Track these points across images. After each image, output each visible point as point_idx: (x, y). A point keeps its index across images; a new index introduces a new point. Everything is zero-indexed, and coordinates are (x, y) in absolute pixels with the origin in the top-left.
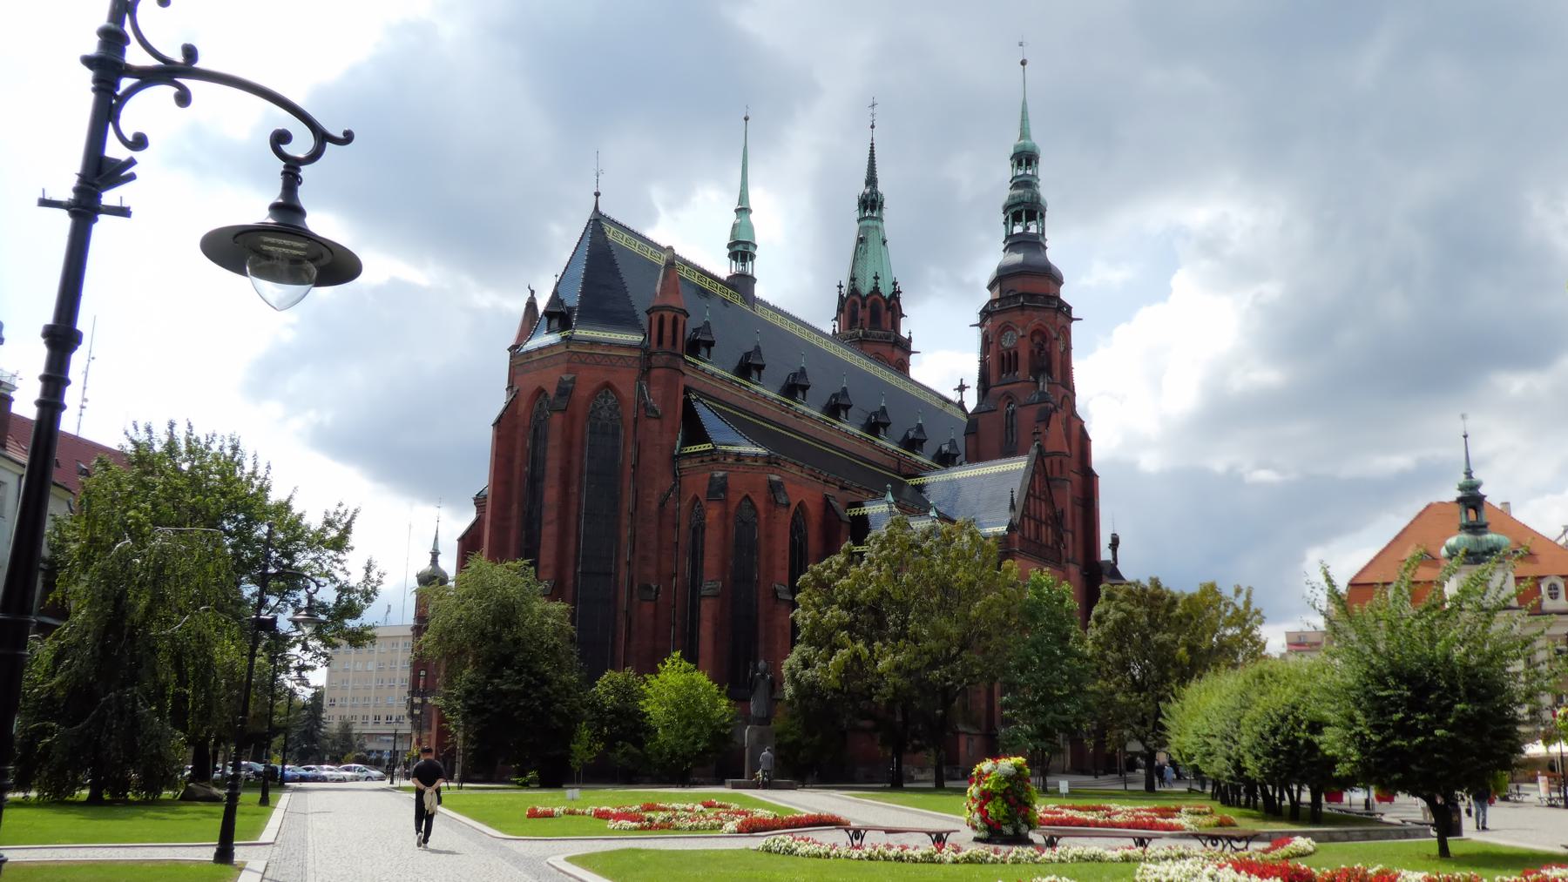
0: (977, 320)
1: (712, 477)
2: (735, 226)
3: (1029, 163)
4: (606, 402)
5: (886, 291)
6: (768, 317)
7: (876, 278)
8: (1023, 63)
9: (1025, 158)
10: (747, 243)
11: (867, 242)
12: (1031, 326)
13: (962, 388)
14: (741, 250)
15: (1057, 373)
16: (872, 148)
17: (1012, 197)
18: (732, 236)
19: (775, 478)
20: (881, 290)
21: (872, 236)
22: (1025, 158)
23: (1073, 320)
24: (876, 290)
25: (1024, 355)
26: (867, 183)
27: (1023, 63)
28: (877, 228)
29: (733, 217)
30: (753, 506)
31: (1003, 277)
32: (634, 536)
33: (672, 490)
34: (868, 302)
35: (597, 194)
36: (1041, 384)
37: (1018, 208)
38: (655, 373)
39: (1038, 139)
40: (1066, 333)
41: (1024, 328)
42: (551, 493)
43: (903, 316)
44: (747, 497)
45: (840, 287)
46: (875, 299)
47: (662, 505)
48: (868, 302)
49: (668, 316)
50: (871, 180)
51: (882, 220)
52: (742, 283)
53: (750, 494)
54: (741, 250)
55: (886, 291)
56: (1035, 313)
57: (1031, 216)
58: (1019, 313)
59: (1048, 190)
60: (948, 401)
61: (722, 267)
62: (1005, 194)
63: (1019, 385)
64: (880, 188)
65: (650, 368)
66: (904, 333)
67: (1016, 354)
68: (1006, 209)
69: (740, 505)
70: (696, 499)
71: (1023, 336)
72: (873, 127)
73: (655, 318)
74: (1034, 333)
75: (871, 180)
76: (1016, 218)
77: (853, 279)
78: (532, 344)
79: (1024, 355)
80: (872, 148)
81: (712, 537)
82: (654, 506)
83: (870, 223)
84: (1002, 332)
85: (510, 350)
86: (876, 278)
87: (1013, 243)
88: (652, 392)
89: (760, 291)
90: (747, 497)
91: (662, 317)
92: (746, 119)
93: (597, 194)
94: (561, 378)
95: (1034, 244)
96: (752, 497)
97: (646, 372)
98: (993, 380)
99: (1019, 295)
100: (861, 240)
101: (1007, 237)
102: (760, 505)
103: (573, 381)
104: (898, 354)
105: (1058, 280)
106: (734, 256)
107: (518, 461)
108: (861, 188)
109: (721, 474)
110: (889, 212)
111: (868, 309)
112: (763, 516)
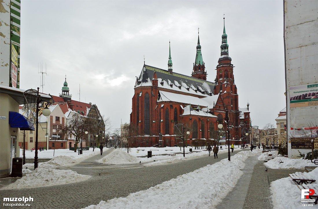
3: (225, 38)
5: (202, 64)
6: (175, 75)
7: (199, 62)
9: (224, 37)
10: (171, 64)
14: (170, 65)
16: (199, 38)
17: (222, 45)
18: (168, 63)
19: (171, 104)
22: (224, 37)
27: (224, 18)
31: (220, 61)
32: (152, 114)
35: (144, 62)
40: (232, 70)
42: (140, 109)
44: (167, 107)
45: (194, 64)
50: (199, 43)
51: (201, 51)
52: (170, 71)
54: (170, 65)
55: (202, 64)
57: (225, 49)
59: (229, 42)
60: (213, 83)
61: (167, 68)
62: (220, 44)
64: (200, 45)
66: (205, 71)
68: (221, 47)
69: (166, 109)
73: (153, 82)
74: (225, 71)
75: (199, 43)
77: (195, 63)
78: (136, 87)
79: (223, 75)
80: (199, 38)
81: (162, 113)
83: (198, 51)
87: (222, 54)
89: (173, 71)
90: (167, 107)
92: (170, 42)
93: (144, 62)
95: (227, 53)
97: (152, 90)
100: (197, 55)
101: (221, 53)
102: (169, 108)
104: (204, 75)
106: (169, 66)
107: (136, 104)
108: (197, 45)
110: (202, 49)
112: (169, 110)
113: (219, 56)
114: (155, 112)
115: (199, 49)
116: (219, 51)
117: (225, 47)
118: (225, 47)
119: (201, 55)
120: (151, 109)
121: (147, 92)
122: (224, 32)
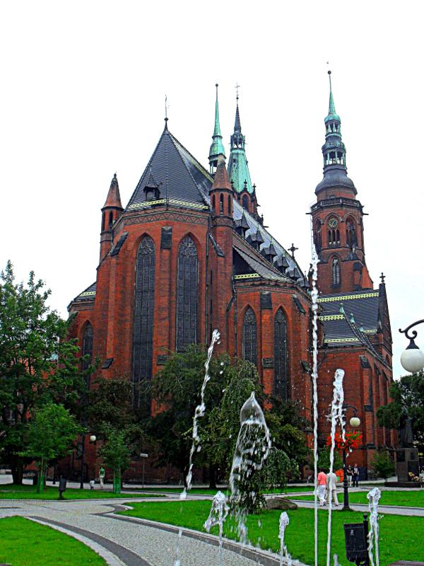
0: (310, 211)
1: (261, 294)
2: (213, 146)
4: (188, 245)
5: (250, 191)
7: (246, 183)
8: (329, 73)
9: (333, 124)
11: (238, 162)
12: (346, 216)
13: (293, 249)
15: (360, 244)
16: (237, 110)
19: (295, 296)
20: (248, 190)
21: (240, 158)
22: (333, 124)
23: (363, 214)
24: (245, 189)
25: (343, 232)
26: (235, 129)
27: (329, 73)
28: (243, 154)
29: (211, 141)
30: (284, 313)
33: (232, 301)
34: (241, 196)
35: (166, 119)
36: (354, 249)
37: (333, 150)
38: (219, 228)
39: (340, 113)
41: (342, 217)
43: (258, 205)
46: (245, 195)
47: (227, 310)
48: (241, 196)
49: (218, 195)
53: (283, 306)
56: (348, 209)
58: (339, 208)
63: (341, 249)
64: (243, 132)
65: (215, 226)
67: (338, 231)
68: (324, 149)
70: (249, 307)
71: (342, 222)
72: (237, 98)
74: (348, 220)
76: (332, 156)
79: (343, 232)
80: (237, 110)
82: (223, 311)
84: (329, 219)
85: (102, 210)
86: (246, 183)
88: (218, 241)
90: (281, 307)
91: (222, 195)
93: (166, 119)
94: (163, 230)
95: (343, 169)
96: (284, 307)
98: (325, 245)
99: (339, 198)
101: (326, 166)
102: (289, 313)
103: (171, 230)
105: (356, 193)
107: (129, 279)
109: (267, 292)
111: (241, 200)
112: (290, 319)
113: (318, 177)
114: (228, 324)
115: (235, 146)
116: (318, 162)
117: (334, 150)
118: (334, 150)
119: (247, 162)
120: (204, 309)
121: (190, 235)
122: (331, 111)
